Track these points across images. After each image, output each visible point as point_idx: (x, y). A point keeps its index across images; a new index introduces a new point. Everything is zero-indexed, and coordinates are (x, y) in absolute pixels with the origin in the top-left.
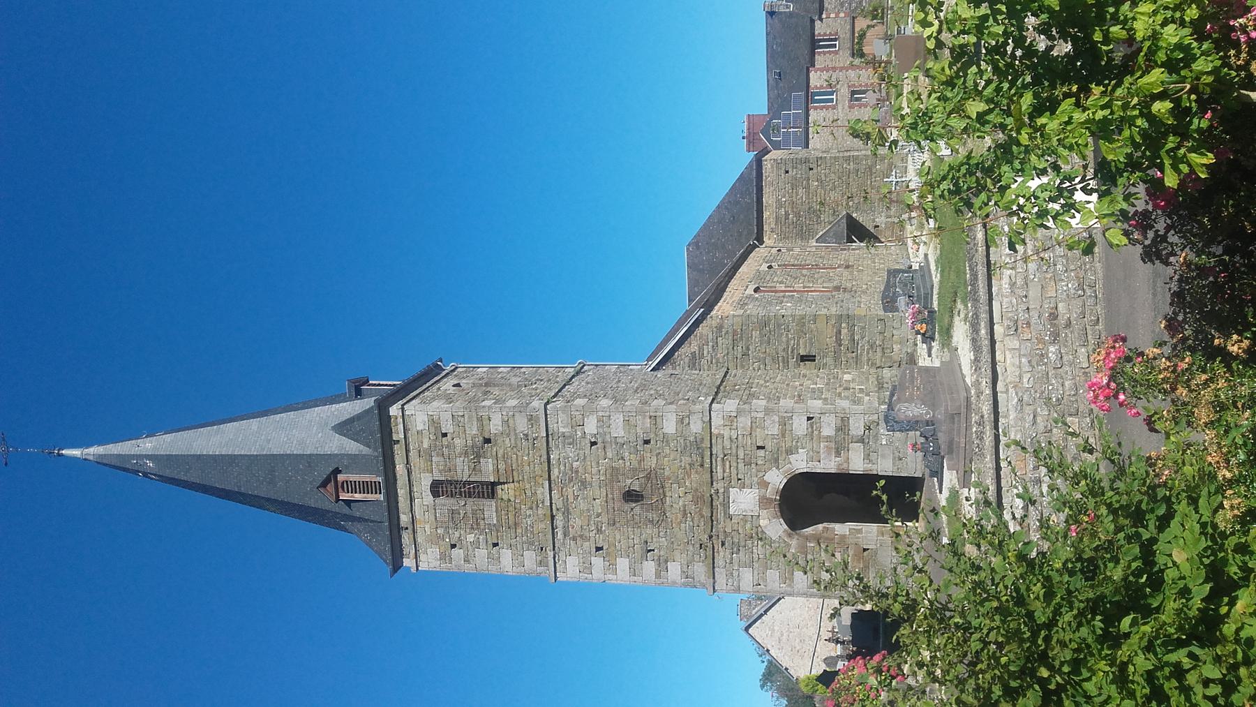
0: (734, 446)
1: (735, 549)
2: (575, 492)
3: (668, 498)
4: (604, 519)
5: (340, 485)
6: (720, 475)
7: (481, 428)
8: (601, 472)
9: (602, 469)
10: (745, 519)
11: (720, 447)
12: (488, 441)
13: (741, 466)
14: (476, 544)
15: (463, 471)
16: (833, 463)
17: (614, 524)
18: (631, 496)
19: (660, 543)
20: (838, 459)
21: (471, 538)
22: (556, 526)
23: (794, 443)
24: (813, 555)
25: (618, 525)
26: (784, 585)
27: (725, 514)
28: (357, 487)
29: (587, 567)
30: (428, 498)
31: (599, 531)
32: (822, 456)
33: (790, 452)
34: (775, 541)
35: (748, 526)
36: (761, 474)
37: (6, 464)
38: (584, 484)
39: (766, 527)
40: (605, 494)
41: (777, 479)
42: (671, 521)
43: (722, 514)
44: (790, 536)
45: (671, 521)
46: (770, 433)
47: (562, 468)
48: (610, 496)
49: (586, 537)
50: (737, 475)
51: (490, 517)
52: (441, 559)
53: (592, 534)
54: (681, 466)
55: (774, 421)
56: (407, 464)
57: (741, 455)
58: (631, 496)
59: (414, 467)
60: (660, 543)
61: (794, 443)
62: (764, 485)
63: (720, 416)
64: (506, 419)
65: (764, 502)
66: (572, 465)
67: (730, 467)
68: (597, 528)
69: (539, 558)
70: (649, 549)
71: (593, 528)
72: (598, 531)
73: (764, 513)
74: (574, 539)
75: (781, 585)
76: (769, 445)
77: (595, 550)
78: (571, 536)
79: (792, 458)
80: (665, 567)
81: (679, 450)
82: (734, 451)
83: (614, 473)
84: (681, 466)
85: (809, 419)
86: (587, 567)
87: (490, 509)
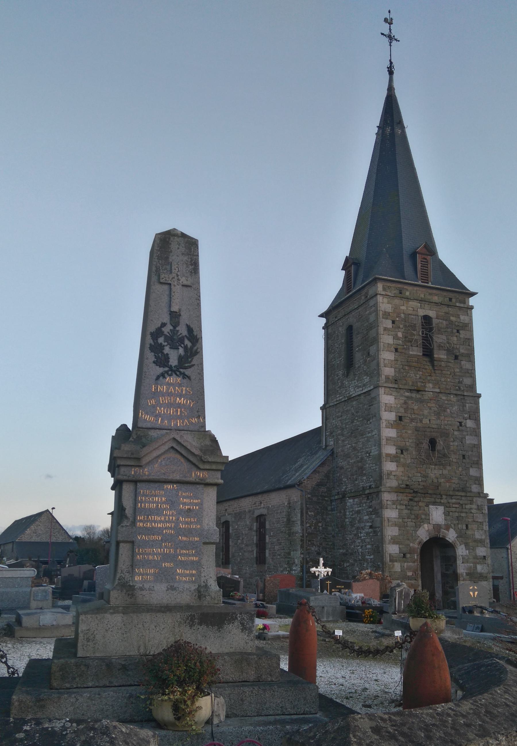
0: (467, 510)
1: (409, 507)
2: (433, 408)
3: (434, 466)
4: (419, 425)
5: (425, 257)
6: (450, 501)
7: (462, 355)
8: (445, 426)
9: (447, 427)
10: (428, 515)
11: (466, 502)
12: (456, 358)
13: (457, 514)
14: (396, 337)
15: (439, 339)
16: (462, 571)
17: (416, 430)
18: (433, 443)
19: (407, 459)
20: (465, 574)
21: (400, 335)
22: (412, 392)
23: (471, 548)
24: (278, 550)
25: (416, 433)
26: (390, 538)
27: (429, 502)
28: (425, 268)
29: (389, 409)
30: (422, 313)
31: (412, 420)
32: (466, 565)
33: (467, 545)
34: (416, 533)
35: (423, 517)
36: (452, 525)
37: (389, 12)
38: (438, 414)
39: (424, 527)
40: (434, 427)
41: (451, 536)
42: (421, 467)
43: (428, 501)
44: (420, 543)
45: (421, 467)
46: (476, 533)
47: (446, 402)
48: (432, 430)
49: (407, 411)
50: (452, 512)
51: (412, 351)
52: (385, 312)
53: (409, 415)
54: (453, 477)
55: (482, 536)
56: (441, 304)
57: (463, 515)
58: (433, 443)
59: (439, 308)
60: (407, 459)
61: (471, 548)
62: (447, 527)
63: (482, 503)
64: (469, 372)
65: (437, 527)
66: (448, 408)
67: (456, 508)
68: (414, 419)
69: (391, 377)
70: (404, 451)
71: (413, 416)
72: (411, 419)
73: (431, 527)
74: (405, 403)
75: (390, 537)
76: (469, 532)
77: (400, 415)
78: (407, 401)
79: (463, 546)
80: (393, 460)
81: (461, 477)
82: (464, 510)
83: (445, 434)
84: (453, 477)
85: (484, 557)
86: (389, 409)
87: (416, 351)
